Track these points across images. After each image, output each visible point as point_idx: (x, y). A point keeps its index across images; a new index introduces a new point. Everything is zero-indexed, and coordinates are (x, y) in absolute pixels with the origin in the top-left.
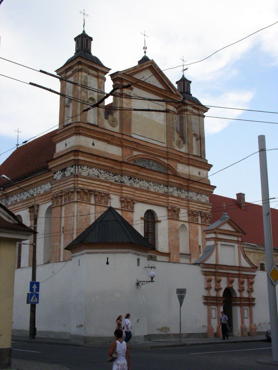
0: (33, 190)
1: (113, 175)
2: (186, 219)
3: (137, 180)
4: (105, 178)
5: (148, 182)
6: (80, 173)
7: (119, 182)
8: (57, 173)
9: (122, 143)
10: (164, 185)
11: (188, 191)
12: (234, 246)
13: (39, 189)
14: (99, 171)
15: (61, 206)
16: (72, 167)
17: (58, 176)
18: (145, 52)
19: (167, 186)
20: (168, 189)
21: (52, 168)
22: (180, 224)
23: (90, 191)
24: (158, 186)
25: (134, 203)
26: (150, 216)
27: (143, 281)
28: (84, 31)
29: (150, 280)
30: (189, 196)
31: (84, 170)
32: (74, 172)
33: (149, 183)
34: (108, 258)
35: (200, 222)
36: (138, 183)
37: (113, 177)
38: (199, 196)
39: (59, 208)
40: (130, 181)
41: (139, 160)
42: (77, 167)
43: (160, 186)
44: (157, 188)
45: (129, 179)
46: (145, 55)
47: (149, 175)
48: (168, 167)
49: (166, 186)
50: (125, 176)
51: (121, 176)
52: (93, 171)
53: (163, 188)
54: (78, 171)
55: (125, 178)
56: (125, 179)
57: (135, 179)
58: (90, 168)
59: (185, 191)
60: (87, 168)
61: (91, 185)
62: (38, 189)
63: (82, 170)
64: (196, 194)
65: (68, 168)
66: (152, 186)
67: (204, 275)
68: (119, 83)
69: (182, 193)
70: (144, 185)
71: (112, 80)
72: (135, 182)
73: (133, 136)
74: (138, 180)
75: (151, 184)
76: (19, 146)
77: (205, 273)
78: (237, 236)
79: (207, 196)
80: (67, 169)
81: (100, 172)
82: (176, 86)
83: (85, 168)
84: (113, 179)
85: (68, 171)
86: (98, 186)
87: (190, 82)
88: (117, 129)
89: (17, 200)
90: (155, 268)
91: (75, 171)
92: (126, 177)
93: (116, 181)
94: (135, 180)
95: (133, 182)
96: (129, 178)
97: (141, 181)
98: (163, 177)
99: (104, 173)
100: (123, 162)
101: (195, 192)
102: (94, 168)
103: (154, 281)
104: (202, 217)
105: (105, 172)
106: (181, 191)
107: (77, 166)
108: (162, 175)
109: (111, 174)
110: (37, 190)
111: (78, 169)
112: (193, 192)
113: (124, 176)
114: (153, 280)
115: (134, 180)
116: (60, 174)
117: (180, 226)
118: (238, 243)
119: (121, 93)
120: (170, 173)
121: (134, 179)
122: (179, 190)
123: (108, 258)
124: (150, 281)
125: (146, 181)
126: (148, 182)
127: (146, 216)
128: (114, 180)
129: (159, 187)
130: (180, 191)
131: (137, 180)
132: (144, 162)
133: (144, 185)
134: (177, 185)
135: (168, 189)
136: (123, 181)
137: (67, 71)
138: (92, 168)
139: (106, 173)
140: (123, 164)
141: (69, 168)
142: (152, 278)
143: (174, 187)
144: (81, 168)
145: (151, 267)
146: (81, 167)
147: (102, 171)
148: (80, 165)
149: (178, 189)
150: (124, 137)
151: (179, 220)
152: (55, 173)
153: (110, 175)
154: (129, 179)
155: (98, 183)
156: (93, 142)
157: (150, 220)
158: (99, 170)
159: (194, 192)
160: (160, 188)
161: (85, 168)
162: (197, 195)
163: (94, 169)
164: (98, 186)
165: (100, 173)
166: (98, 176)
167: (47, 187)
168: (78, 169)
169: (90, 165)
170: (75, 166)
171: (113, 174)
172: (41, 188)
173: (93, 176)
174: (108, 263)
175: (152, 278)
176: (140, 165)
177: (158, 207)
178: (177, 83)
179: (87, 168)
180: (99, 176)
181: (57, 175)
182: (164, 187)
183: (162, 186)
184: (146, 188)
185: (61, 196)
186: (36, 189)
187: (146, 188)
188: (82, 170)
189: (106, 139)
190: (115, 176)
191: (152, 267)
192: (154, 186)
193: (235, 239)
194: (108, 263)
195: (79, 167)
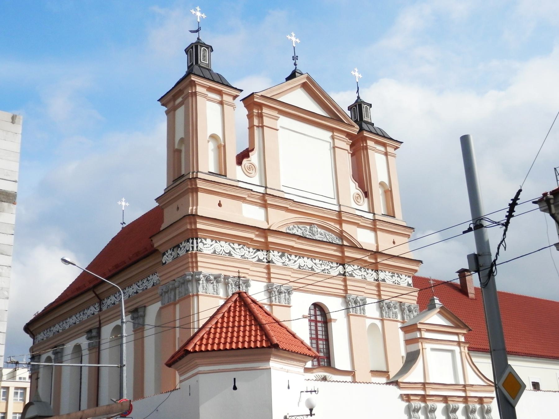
0: (137, 285)
2: (377, 314)
3: (293, 257)
4: (242, 256)
5: (312, 260)
6: (200, 251)
7: (264, 262)
8: (167, 254)
9: (265, 201)
10: (337, 263)
11: (378, 271)
12: (452, 351)
13: (145, 282)
14: (230, 246)
15: (175, 304)
16: (188, 241)
17: (167, 258)
18: (295, 64)
19: (343, 265)
20: (345, 269)
21: (158, 246)
22: (368, 322)
23: (217, 278)
24: (328, 265)
25: (289, 293)
26: (318, 313)
27: (298, 416)
28: (198, 39)
29: (309, 413)
30: (380, 279)
31: (207, 246)
32: (191, 249)
33: (314, 260)
34: (235, 379)
35: (399, 318)
36: (295, 261)
38: (395, 278)
39: (172, 307)
40: (282, 258)
41: (296, 226)
42: (195, 241)
43: (332, 265)
45: (281, 257)
46: (296, 68)
48: (341, 235)
49: (340, 264)
50: (273, 251)
51: (267, 251)
52: (221, 246)
54: (197, 247)
55: (274, 255)
56: (275, 256)
57: (291, 255)
58: (216, 242)
59: (372, 270)
60: (212, 242)
62: (143, 283)
63: (204, 244)
64: (390, 274)
65: (181, 243)
66: (319, 265)
67: (403, 400)
68: (255, 111)
69: (367, 274)
70: (305, 265)
71: (246, 106)
72: (290, 260)
73: (282, 189)
74: (296, 256)
75: (317, 261)
76: (124, 226)
77: (407, 398)
78: (457, 334)
79: (409, 277)
80: (181, 246)
81: (232, 247)
82: (349, 113)
83: (209, 241)
84: (254, 258)
85: (182, 249)
87: (370, 105)
88: (256, 180)
89: (115, 302)
90: (317, 392)
91: (193, 247)
92: (276, 253)
93: (259, 260)
94: (290, 258)
95: (287, 260)
96: (280, 254)
97: (300, 258)
98: (335, 251)
100: (269, 230)
101: (389, 272)
102: (222, 241)
103: (314, 415)
104: (402, 311)
105: (241, 246)
106: (366, 271)
107: (195, 239)
108: (335, 248)
109: (251, 250)
110: (142, 284)
111: (197, 243)
113: (271, 251)
114: (313, 413)
115: (288, 258)
116: (171, 255)
117: (367, 326)
118: (460, 346)
119: (260, 125)
120: (345, 243)
121: (289, 256)
122: (363, 270)
123: (235, 379)
124: (307, 415)
125: (308, 258)
126: (312, 258)
127: (312, 312)
128: (257, 258)
129: (330, 266)
130: (364, 271)
131: (293, 257)
132: (303, 229)
133: (305, 264)
135: (345, 269)
136: (271, 259)
137: (175, 97)
138: (220, 241)
139: (243, 248)
141: (184, 244)
142: (311, 410)
144: (201, 242)
145: (311, 392)
146: (202, 240)
147: (236, 246)
148: (200, 238)
149: (361, 268)
150: (269, 191)
151: (365, 317)
152: (164, 254)
153: (249, 252)
154: (281, 257)
156: (220, 201)
157: (319, 318)
158: (232, 244)
159: (387, 272)
161: (209, 241)
162: (392, 276)
163: (223, 243)
165: (233, 248)
166: (230, 254)
167: (155, 278)
168: (197, 243)
169: (217, 237)
170: (193, 239)
172: (147, 280)
173: (221, 254)
174: (235, 388)
175: (311, 410)
176: (297, 233)
178: (350, 108)
179: (212, 242)
180: (232, 253)
181: (167, 256)
182: (338, 266)
183: (335, 265)
185: (175, 289)
186: (141, 283)
188: (204, 244)
190: (258, 253)
191: (313, 390)
193: (455, 338)
194: (235, 388)
195: (199, 240)
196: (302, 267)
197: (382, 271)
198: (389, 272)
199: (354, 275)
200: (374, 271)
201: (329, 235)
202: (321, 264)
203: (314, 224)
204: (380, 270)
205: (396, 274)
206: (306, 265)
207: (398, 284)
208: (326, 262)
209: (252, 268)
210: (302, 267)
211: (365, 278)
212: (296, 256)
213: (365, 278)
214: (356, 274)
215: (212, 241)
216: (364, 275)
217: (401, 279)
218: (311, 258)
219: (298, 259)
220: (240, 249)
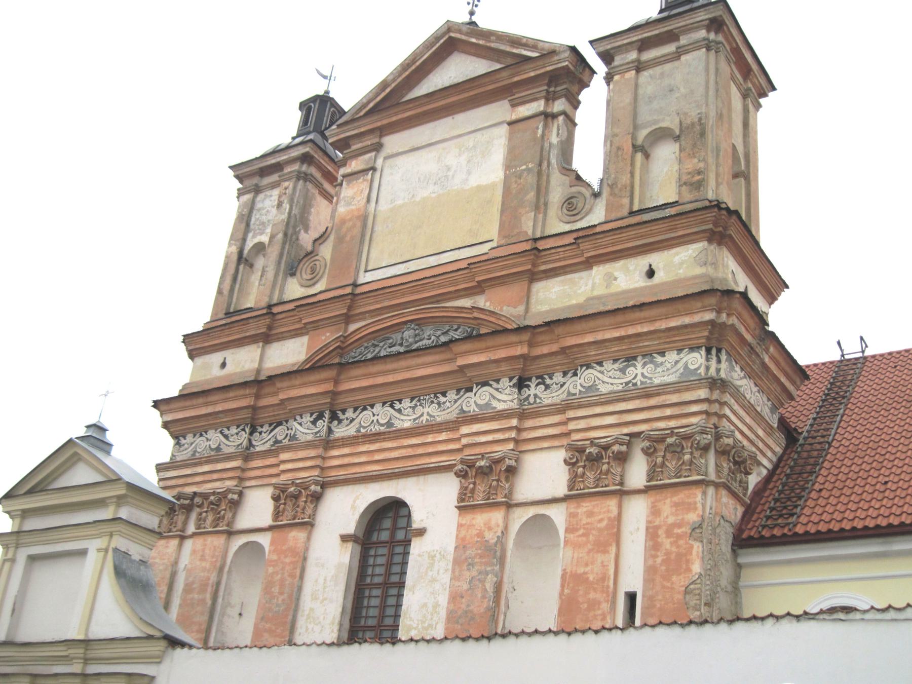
1: (272, 427)
4: (238, 445)
5: (392, 406)
24: (432, 402)
36: (353, 420)
37: (270, 433)
44: (426, 410)
47: (380, 380)
53: (456, 401)
58: (201, 435)
59: (565, 374)
61: (190, 480)
74: (355, 409)
79: (692, 349)
84: (267, 442)
86: (207, 477)
97: (365, 409)
105: (241, 427)
112: (600, 364)
131: (350, 414)
134: (504, 367)
139: (244, 430)
140: (279, 385)
143: (498, 381)
155: (206, 468)
156: (225, 358)
160: (439, 404)
164: (207, 477)
171: (270, 425)
177: (421, 478)
184: (382, 425)
187: (382, 425)
189: (253, 333)
192: (414, 408)
197: (588, 366)
199: (495, 403)
200: (570, 375)
204: (582, 366)
206: (375, 421)
207: (642, 383)
208: (428, 397)
210: (364, 428)
212: (355, 409)
214: (499, 400)
215: (195, 435)
216: (536, 396)
218: (392, 401)
219: (360, 413)
220: (237, 434)
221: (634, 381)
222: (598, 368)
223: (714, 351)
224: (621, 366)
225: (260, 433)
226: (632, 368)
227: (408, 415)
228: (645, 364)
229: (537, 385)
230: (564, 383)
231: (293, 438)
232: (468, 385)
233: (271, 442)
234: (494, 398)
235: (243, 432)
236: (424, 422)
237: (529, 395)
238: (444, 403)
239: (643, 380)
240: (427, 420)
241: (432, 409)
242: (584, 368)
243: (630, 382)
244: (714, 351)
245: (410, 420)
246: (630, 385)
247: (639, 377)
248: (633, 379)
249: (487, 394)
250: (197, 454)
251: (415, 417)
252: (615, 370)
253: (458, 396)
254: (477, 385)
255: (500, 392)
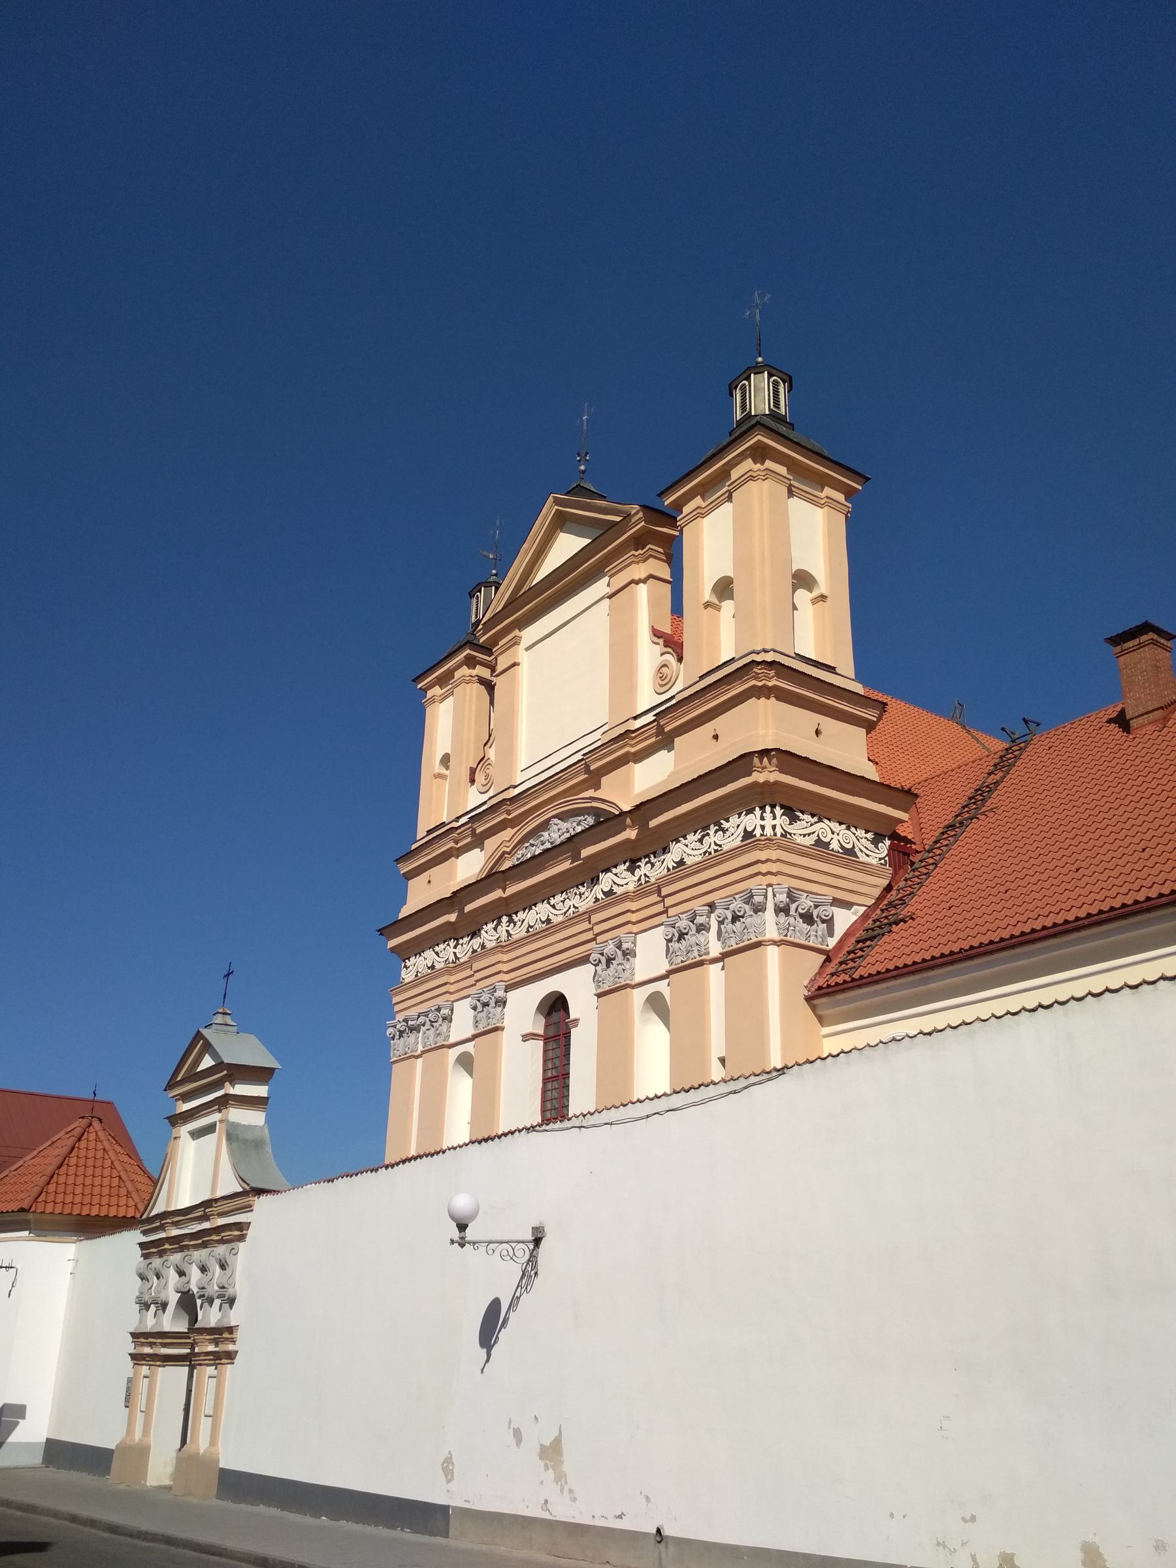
1: (470, 937)
24: (576, 894)
99: (444, 949)
153: (462, 945)
192: (563, 902)
196: (531, 927)
197: (678, 841)
198: (695, 832)
199: (615, 888)
201: (580, 821)
202: (563, 902)
203: (549, 820)
204: (672, 842)
205: (712, 826)
207: (716, 851)
208: (572, 890)
209: (452, 979)
210: (531, 927)
211: (647, 879)
213: (647, 879)
217: (724, 831)
220: (444, 949)
221: (709, 850)
222: (684, 841)
223: (768, 809)
224: (700, 837)
225: (462, 945)
226: (707, 838)
227: (560, 910)
228: (716, 832)
229: (645, 865)
230: (664, 859)
231: (483, 946)
232: (593, 875)
233: (470, 953)
234: (615, 883)
235: (448, 947)
236: (571, 914)
237: (641, 876)
238: (583, 894)
239: (716, 848)
240: (574, 913)
241: (576, 901)
242: (674, 843)
243: (707, 851)
244: (768, 809)
245: (562, 914)
246: (707, 854)
247: (713, 845)
248: (709, 848)
249: (610, 881)
250: (419, 974)
251: (565, 910)
252: (696, 842)
253: (593, 885)
254: (602, 872)
255: (618, 877)
